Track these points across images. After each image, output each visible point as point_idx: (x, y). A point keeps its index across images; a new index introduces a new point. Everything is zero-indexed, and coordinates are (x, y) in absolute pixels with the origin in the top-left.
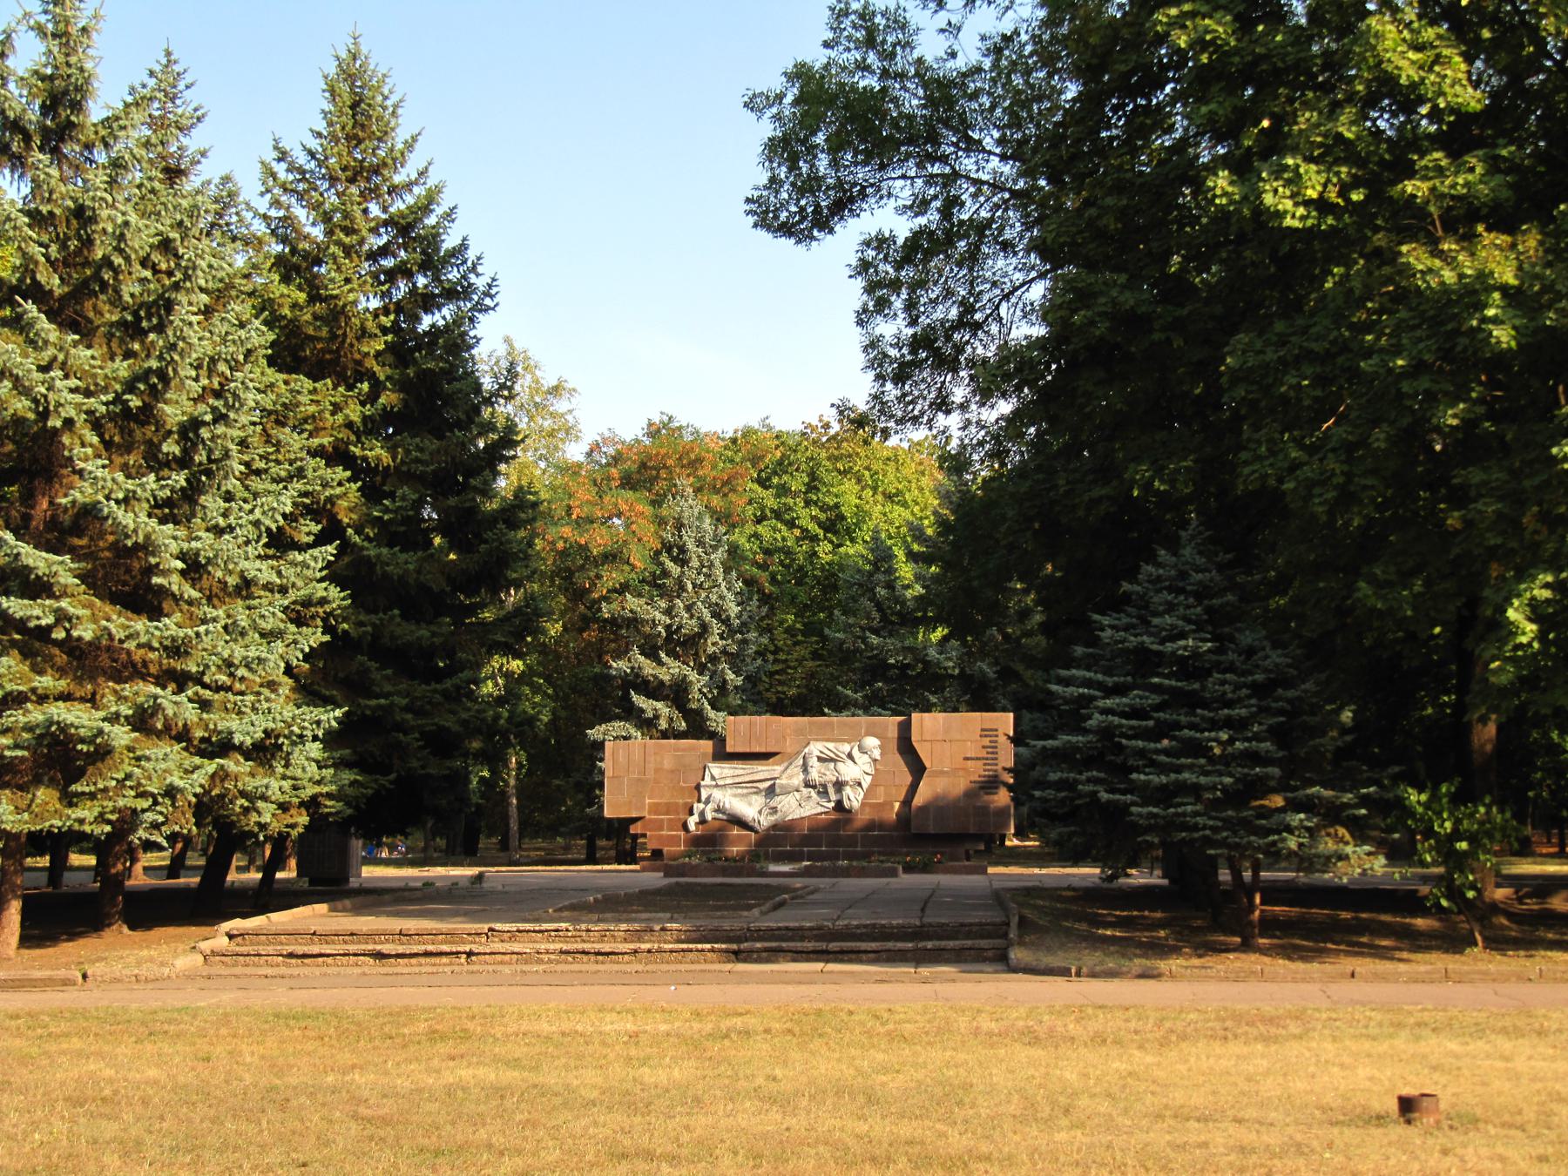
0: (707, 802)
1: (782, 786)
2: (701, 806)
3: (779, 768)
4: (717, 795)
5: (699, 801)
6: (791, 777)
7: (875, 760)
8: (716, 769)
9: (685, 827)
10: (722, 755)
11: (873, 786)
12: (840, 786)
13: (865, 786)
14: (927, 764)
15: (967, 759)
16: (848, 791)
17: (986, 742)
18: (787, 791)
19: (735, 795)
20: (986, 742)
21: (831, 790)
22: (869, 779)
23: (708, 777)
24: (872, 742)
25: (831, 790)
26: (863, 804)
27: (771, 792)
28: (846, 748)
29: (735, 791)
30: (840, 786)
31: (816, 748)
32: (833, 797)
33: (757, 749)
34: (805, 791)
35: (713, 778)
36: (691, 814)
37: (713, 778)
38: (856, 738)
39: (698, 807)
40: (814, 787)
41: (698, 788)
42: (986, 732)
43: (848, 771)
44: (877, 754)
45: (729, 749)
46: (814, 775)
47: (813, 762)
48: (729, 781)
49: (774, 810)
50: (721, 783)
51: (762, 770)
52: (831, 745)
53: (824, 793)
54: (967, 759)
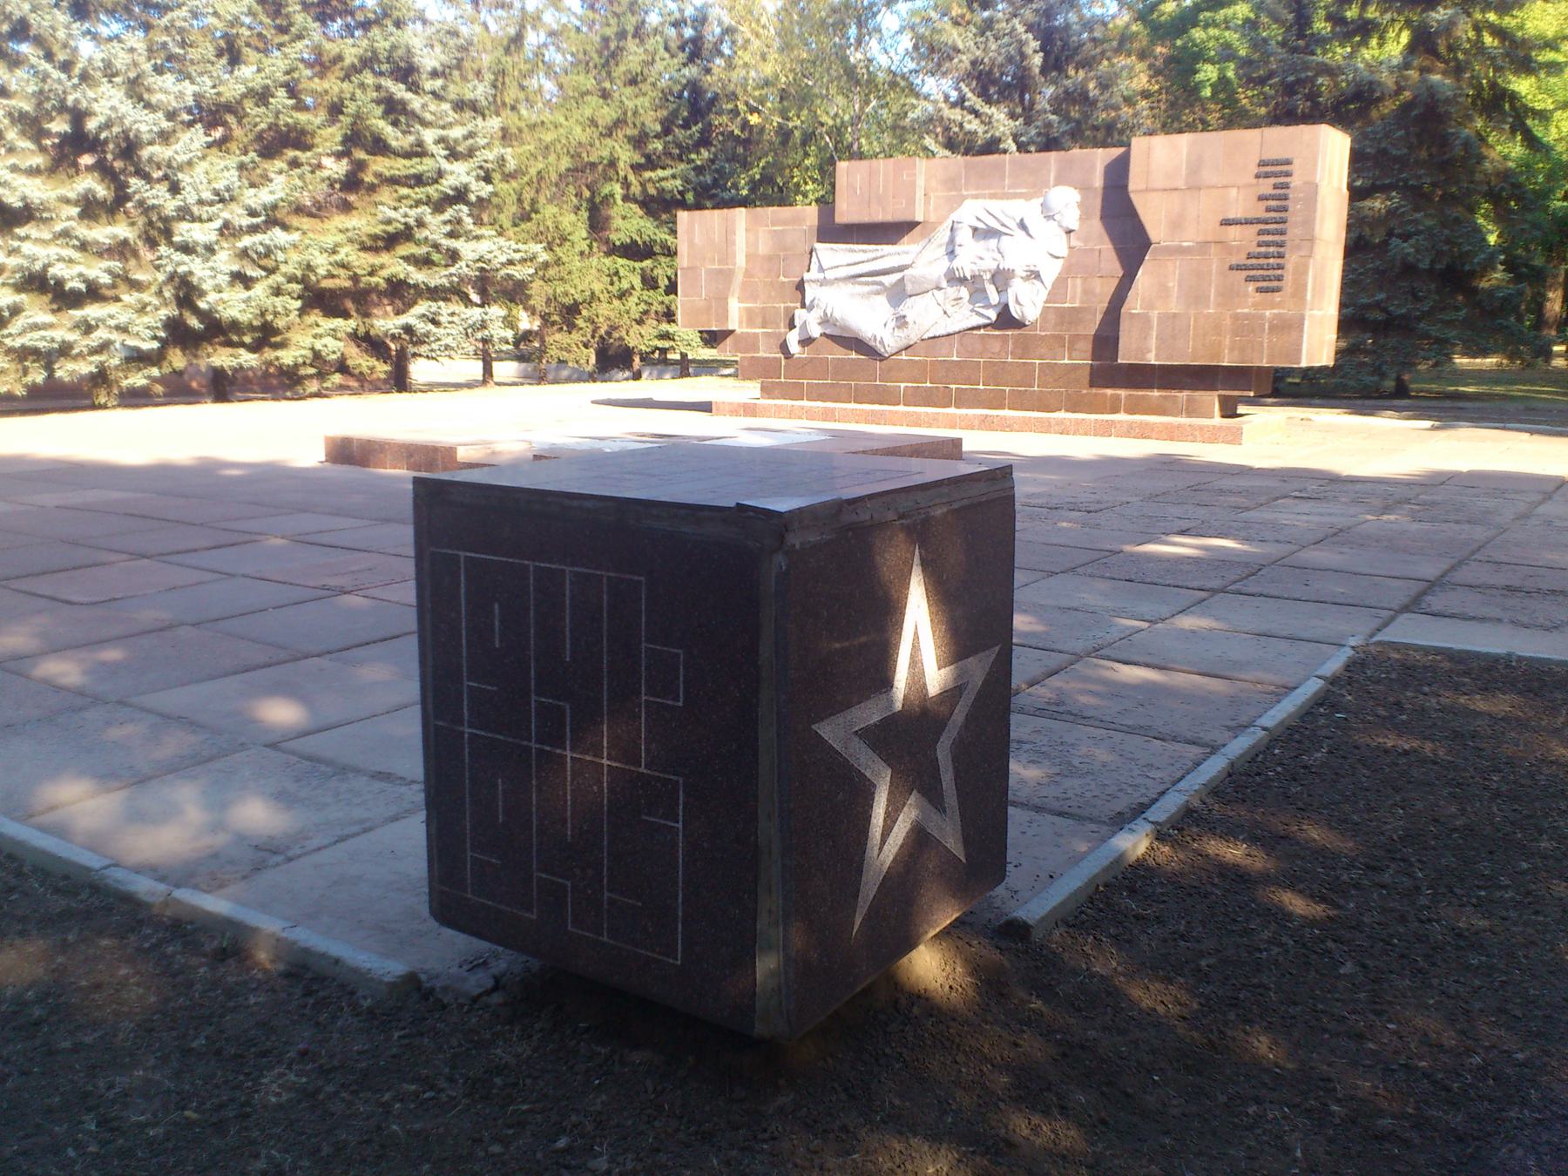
1: (915, 281)
7: (1069, 232)
9: (784, 347)
10: (832, 231)
11: (1060, 283)
12: (1001, 278)
14: (1154, 233)
15: (1226, 223)
17: (1266, 186)
20: (1266, 186)
23: (814, 266)
26: (1045, 310)
27: (898, 295)
29: (850, 288)
31: (972, 211)
32: (994, 298)
33: (880, 216)
34: (952, 292)
35: (821, 269)
36: (792, 326)
37: (821, 269)
39: (801, 315)
40: (962, 281)
41: (800, 287)
43: (1016, 254)
44: (1072, 219)
47: (964, 235)
49: (901, 322)
50: (830, 275)
53: (978, 293)
54: (1226, 223)
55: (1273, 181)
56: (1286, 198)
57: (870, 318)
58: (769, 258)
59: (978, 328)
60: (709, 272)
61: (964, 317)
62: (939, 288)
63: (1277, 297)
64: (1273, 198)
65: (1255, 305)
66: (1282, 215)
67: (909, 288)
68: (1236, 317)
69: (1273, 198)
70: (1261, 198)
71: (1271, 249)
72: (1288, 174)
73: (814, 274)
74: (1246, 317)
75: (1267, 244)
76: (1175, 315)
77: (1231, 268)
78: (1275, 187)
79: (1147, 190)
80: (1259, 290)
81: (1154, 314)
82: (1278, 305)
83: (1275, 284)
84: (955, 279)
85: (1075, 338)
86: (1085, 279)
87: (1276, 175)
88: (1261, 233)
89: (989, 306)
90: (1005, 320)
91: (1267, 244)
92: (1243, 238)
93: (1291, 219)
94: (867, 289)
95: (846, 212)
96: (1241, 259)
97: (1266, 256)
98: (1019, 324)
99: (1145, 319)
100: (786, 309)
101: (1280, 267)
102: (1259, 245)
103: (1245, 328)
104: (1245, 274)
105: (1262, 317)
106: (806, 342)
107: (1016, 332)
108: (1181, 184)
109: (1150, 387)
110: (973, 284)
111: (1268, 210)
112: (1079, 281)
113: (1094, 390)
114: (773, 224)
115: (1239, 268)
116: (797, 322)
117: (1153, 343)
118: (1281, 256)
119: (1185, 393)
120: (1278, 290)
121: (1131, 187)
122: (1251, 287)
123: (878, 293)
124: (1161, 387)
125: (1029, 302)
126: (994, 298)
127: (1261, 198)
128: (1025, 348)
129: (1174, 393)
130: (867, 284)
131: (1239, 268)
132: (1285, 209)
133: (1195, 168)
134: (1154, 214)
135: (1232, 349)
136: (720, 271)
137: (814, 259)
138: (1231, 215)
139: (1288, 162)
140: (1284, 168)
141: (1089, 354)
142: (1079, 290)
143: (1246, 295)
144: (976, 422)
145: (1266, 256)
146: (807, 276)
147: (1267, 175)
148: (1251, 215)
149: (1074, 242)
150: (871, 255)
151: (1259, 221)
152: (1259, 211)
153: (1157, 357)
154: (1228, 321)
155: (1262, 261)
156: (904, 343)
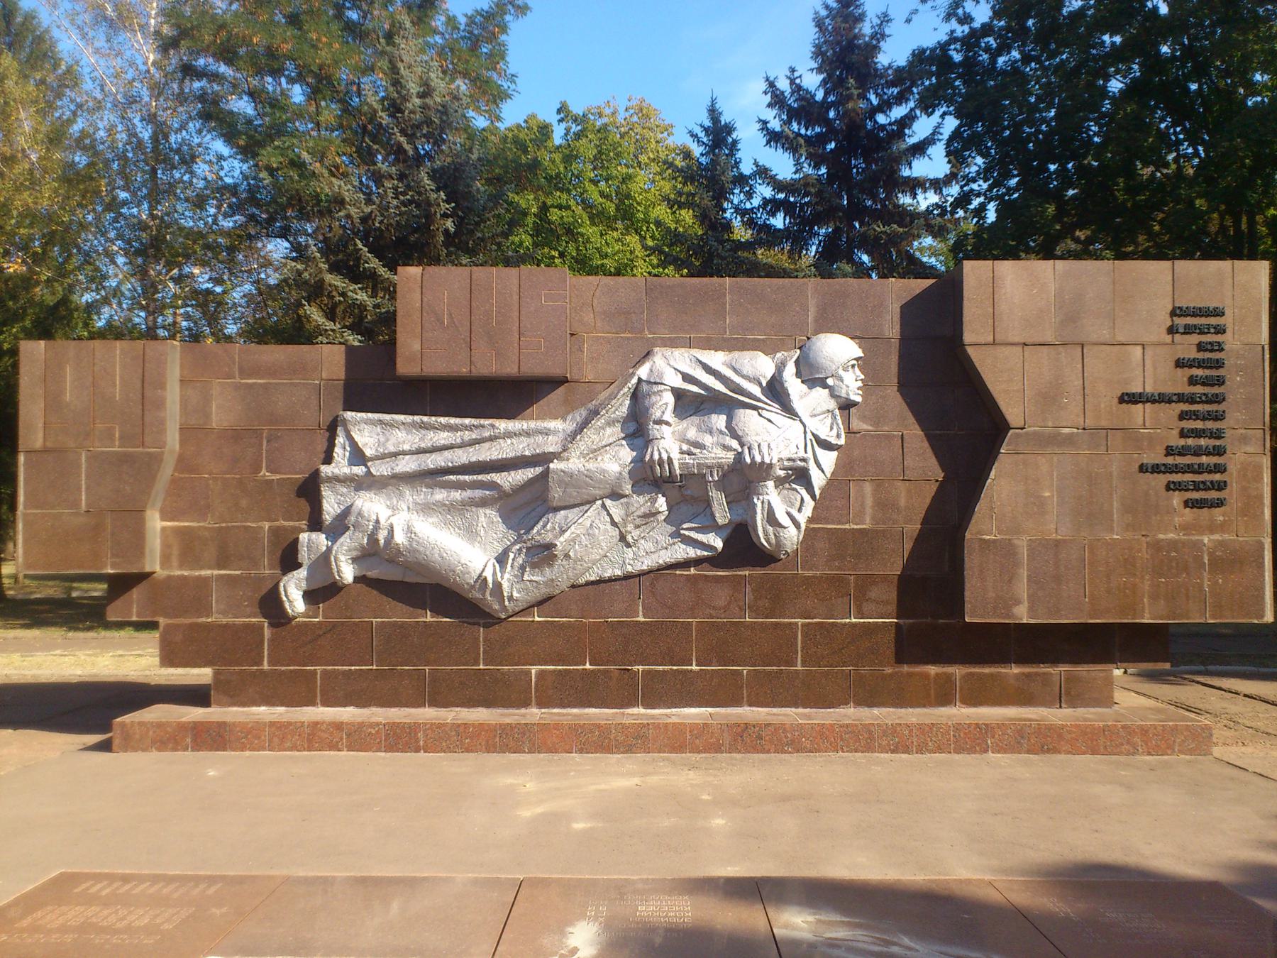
0: (339, 528)
1: (570, 479)
2: (321, 540)
3: (559, 426)
4: (372, 506)
5: (316, 524)
6: (595, 452)
7: (846, 406)
8: (368, 432)
9: (272, 604)
13: (818, 480)
14: (1012, 414)
15: (1129, 399)
16: (772, 496)
18: (586, 494)
19: (427, 509)
20: (1187, 346)
21: (719, 502)
22: (829, 459)
23: (341, 453)
24: (838, 349)
25: (719, 502)
28: (763, 365)
29: (423, 494)
30: (744, 477)
31: (671, 367)
32: (722, 514)
33: (488, 365)
34: (640, 503)
35: (358, 456)
36: (289, 561)
38: (791, 336)
39: (312, 542)
41: (310, 490)
42: (1194, 320)
43: (773, 437)
44: (852, 385)
45: (406, 366)
46: (670, 442)
48: (407, 465)
49: (542, 554)
51: (510, 437)
52: (717, 359)
54: (1129, 399)
55: (1195, 339)
56: (1219, 364)
57: (468, 549)
58: (235, 435)
59: (685, 564)
60: (93, 457)
61: (658, 548)
62: (616, 495)
63: (1218, 514)
64: (1200, 364)
65: (1186, 528)
66: (1216, 390)
67: (556, 494)
68: (1157, 546)
69: (1200, 364)
70: (1180, 364)
71: (1202, 442)
72: (1220, 330)
73: (340, 465)
74: (1173, 544)
75: (1198, 434)
76: (1057, 544)
77: (1143, 469)
78: (1200, 347)
79: (994, 343)
80: (1187, 504)
81: (1022, 543)
82: (1222, 528)
83: (1213, 495)
84: (649, 477)
85: (866, 582)
86: (878, 484)
87: (1201, 331)
88: (1183, 416)
89: (713, 527)
90: (743, 547)
91: (1198, 434)
92: (1161, 425)
93: (1230, 398)
94: (457, 495)
95: (416, 353)
96: (1157, 457)
97: (1197, 452)
98: (761, 557)
99: (1007, 551)
100: (275, 532)
101: (1220, 469)
102: (1183, 434)
103: (1171, 562)
104: (1163, 479)
105: (1198, 546)
106: (323, 591)
107: (759, 571)
108: (1049, 337)
109: (1004, 660)
110: (682, 491)
111: (1193, 381)
112: (868, 488)
113: (906, 668)
114: (243, 373)
115: (1156, 469)
116: (304, 555)
117: (1022, 588)
118: (1219, 451)
119: (1063, 668)
120: (1220, 503)
121: (968, 337)
122: (1177, 499)
123: (483, 503)
124: (1021, 661)
125: (785, 516)
126: (722, 514)
127: (1180, 364)
128: (776, 596)
129: (1044, 669)
130: (461, 486)
131: (1156, 469)
132: (1220, 381)
133: (1071, 314)
134: (1008, 379)
135: (1154, 597)
136: (124, 459)
137: (340, 439)
138: (1136, 389)
139: (1218, 313)
140: (1213, 321)
141: (892, 608)
142: (869, 502)
143: (1171, 511)
144: (727, 738)
145: (1197, 452)
146: (326, 470)
147: (1188, 330)
148: (1169, 389)
149: (856, 424)
150: (468, 435)
151: (1181, 398)
152: (1177, 382)
153: (1032, 610)
154: (1144, 554)
155: (1188, 460)
156: (537, 595)
